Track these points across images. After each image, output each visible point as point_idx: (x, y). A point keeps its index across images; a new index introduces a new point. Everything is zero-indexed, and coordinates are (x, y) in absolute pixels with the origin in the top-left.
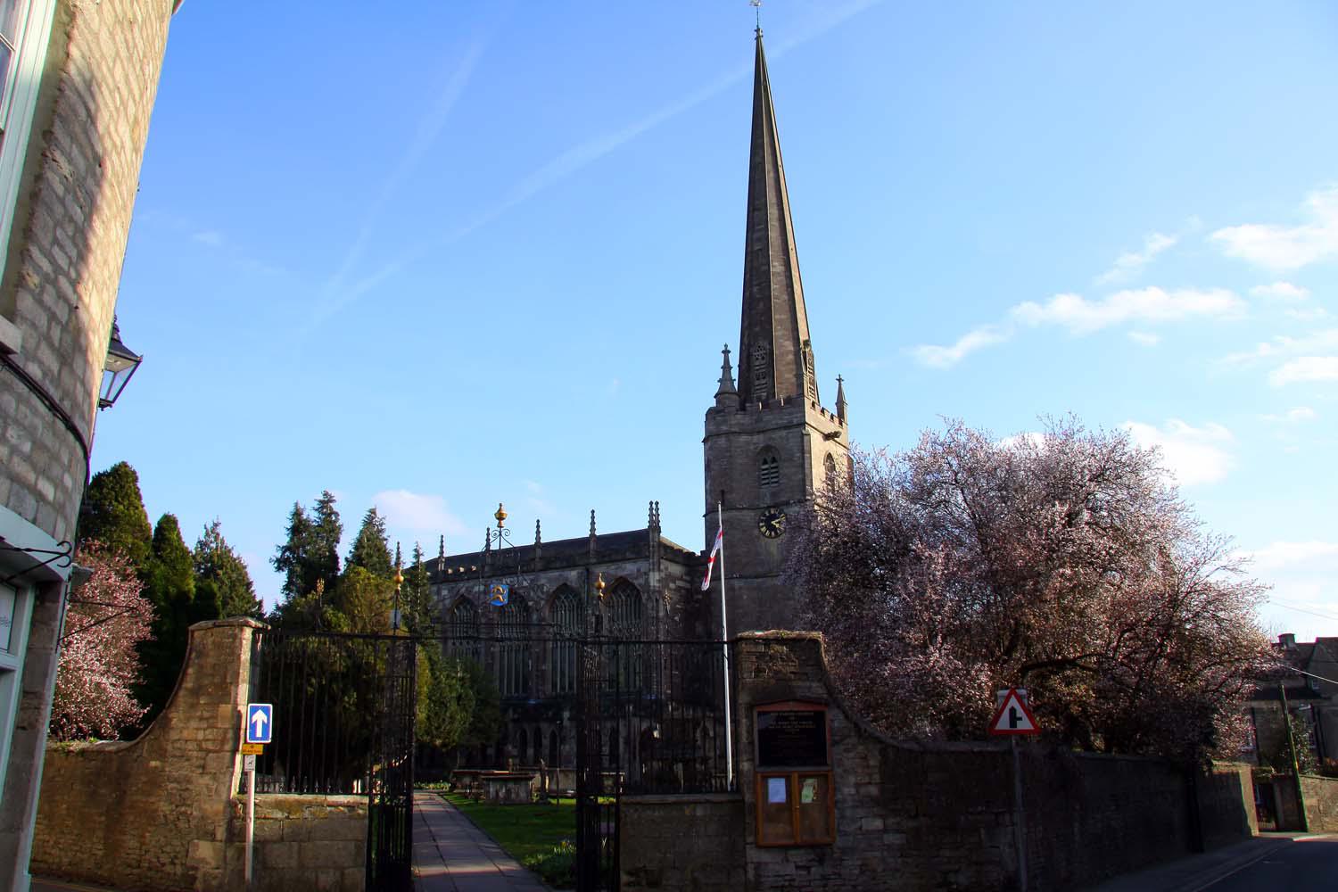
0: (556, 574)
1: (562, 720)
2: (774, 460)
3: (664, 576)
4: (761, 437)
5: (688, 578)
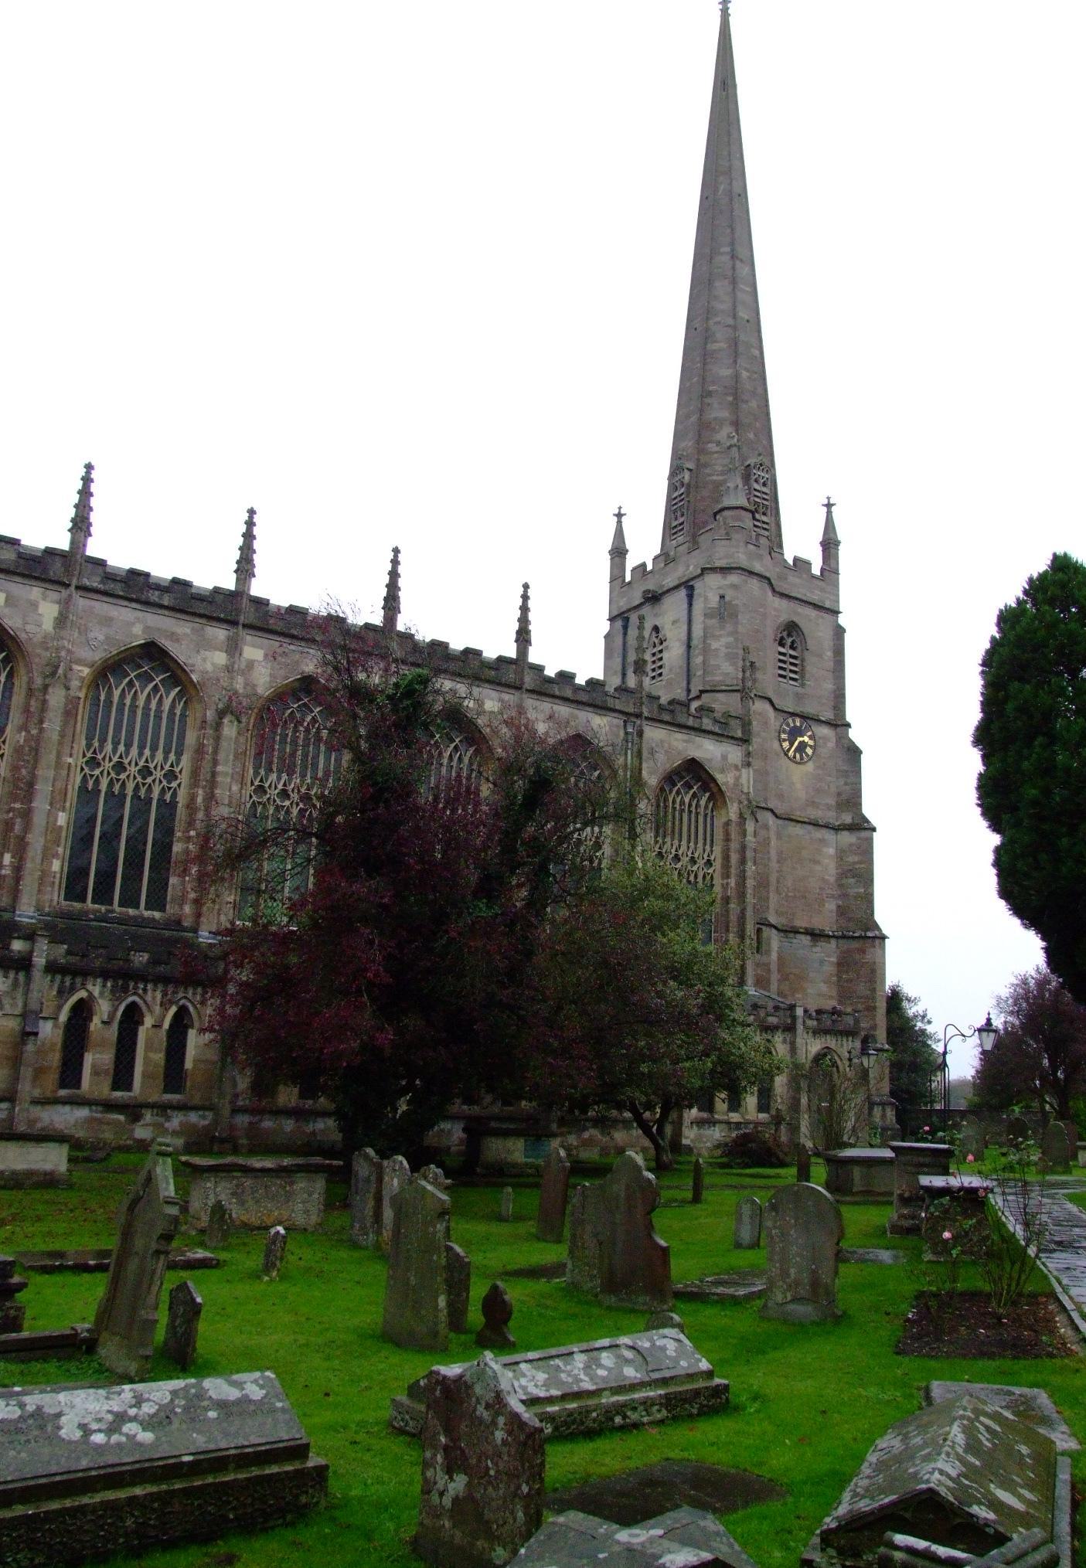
0: (563, 710)
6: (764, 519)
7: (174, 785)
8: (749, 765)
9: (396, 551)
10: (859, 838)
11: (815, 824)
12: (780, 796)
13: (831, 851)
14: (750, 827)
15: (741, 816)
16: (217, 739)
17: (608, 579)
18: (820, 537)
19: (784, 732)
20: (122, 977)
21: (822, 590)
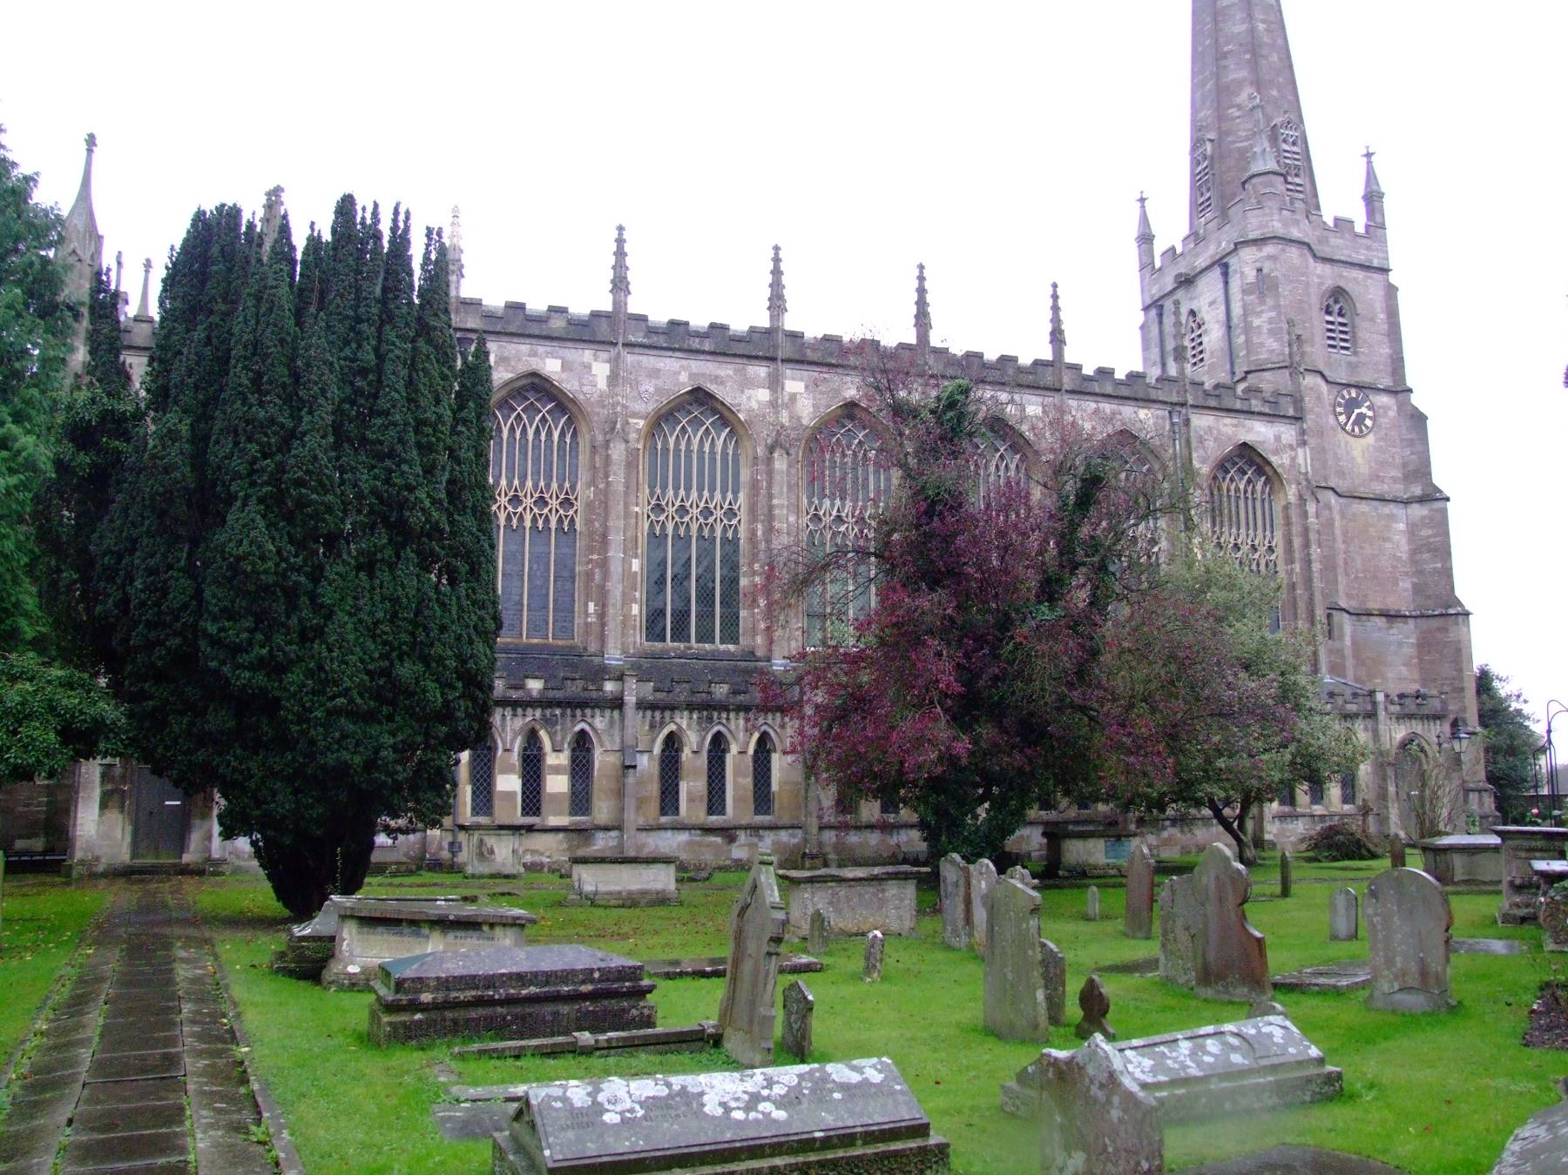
0: (1107, 407)
6: (1298, 180)
7: (734, 522)
8: (1304, 443)
9: (921, 267)
10: (1431, 510)
11: (1382, 500)
12: (1341, 474)
13: (1402, 526)
14: (1311, 508)
15: (1301, 497)
16: (770, 473)
17: (1137, 267)
18: (1361, 191)
19: (1340, 405)
20: (707, 708)
21: (1368, 248)
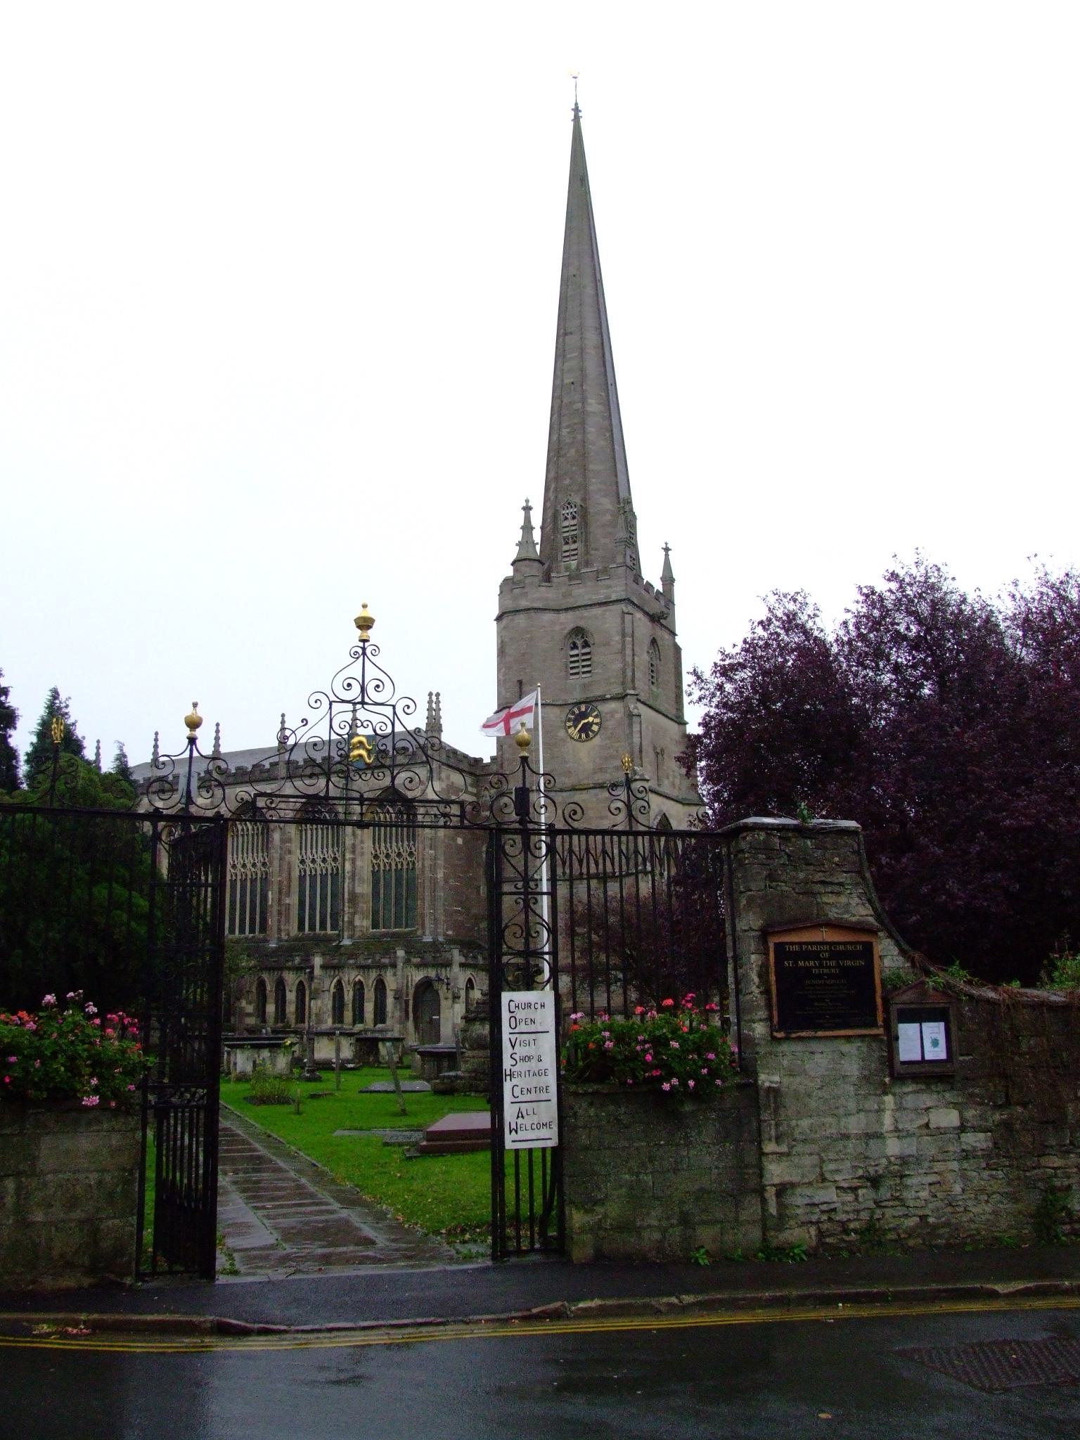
1: (312, 967)
2: (586, 645)
3: (444, 786)
4: (570, 615)
5: (475, 791)
